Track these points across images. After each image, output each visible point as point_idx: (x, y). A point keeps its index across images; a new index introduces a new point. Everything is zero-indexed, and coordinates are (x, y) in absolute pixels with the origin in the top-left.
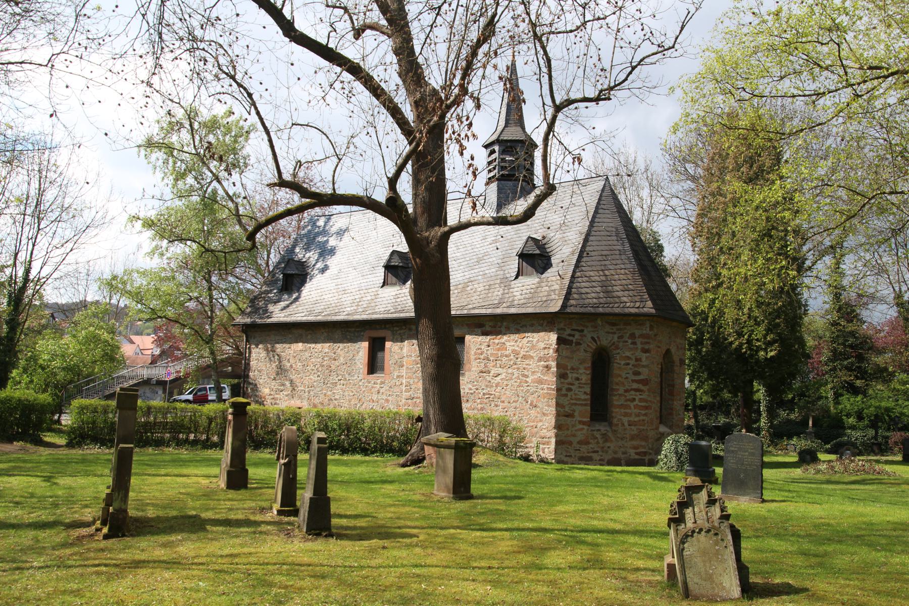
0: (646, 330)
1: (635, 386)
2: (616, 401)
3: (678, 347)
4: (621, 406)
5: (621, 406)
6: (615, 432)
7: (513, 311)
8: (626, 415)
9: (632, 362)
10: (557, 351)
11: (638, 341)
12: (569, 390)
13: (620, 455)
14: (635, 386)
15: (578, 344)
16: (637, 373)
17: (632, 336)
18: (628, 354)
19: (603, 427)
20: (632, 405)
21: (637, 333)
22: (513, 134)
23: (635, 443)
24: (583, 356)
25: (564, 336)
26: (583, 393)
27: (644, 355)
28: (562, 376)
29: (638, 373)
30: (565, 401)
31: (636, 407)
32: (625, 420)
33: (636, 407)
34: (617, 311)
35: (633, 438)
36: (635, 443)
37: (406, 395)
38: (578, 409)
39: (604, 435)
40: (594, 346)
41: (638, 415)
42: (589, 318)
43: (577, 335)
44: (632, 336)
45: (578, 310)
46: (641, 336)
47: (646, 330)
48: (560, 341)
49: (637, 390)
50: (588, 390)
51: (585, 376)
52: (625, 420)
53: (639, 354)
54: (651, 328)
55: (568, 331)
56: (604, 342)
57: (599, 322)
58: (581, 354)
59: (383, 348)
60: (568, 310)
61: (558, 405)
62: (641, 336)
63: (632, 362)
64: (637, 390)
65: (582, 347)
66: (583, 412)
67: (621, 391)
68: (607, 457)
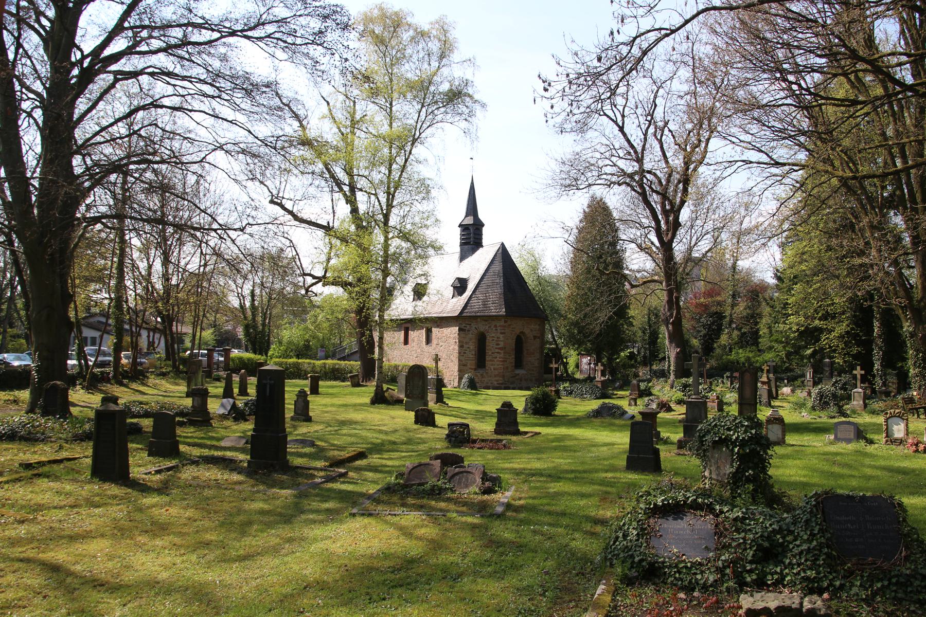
0: (502, 323)
1: (497, 351)
2: (488, 358)
3: (531, 330)
4: (491, 361)
5: (491, 361)
6: (487, 373)
7: (444, 315)
8: (492, 365)
9: (495, 339)
10: (459, 334)
11: (499, 328)
12: (465, 353)
13: (489, 384)
14: (497, 351)
15: (469, 331)
16: (498, 344)
17: (495, 326)
18: (493, 335)
19: (481, 371)
20: (495, 360)
21: (498, 325)
22: (470, 220)
23: (497, 378)
24: (472, 336)
25: (462, 327)
26: (471, 355)
27: (501, 336)
28: (461, 346)
29: (498, 344)
30: (461, 358)
31: (498, 361)
32: (492, 367)
33: (498, 361)
34: (486, 314)
35: (495, 376)
36: (497, 378)
37: (415, 355)
38: (469, 362)
39: (482, 375)
40: (476, 331)
41: (498, 365)
42: (474, 318)
43: (468, 326)
44: (495, 326)
45: (468, 314)
46: (500, 326)
47: (502, 323)
48: (460, 330)
49: (498, 353)
50: (474, 353)
51: (472, 346)
52: (492, 367)
53: (499, 335)
54: (505, 322)
55: (464, 325)
56: (482, 330)
57: (479, 320)
58: (470, 336)
59: (431, 331)
60: (465, 314)
61: (459, 360)
62: (500, 326)
63: (495, 339)
64: (498, 353)
65: (470, 332)
66: (472, 363)
67: (490, 353)
68: (484, 385)
